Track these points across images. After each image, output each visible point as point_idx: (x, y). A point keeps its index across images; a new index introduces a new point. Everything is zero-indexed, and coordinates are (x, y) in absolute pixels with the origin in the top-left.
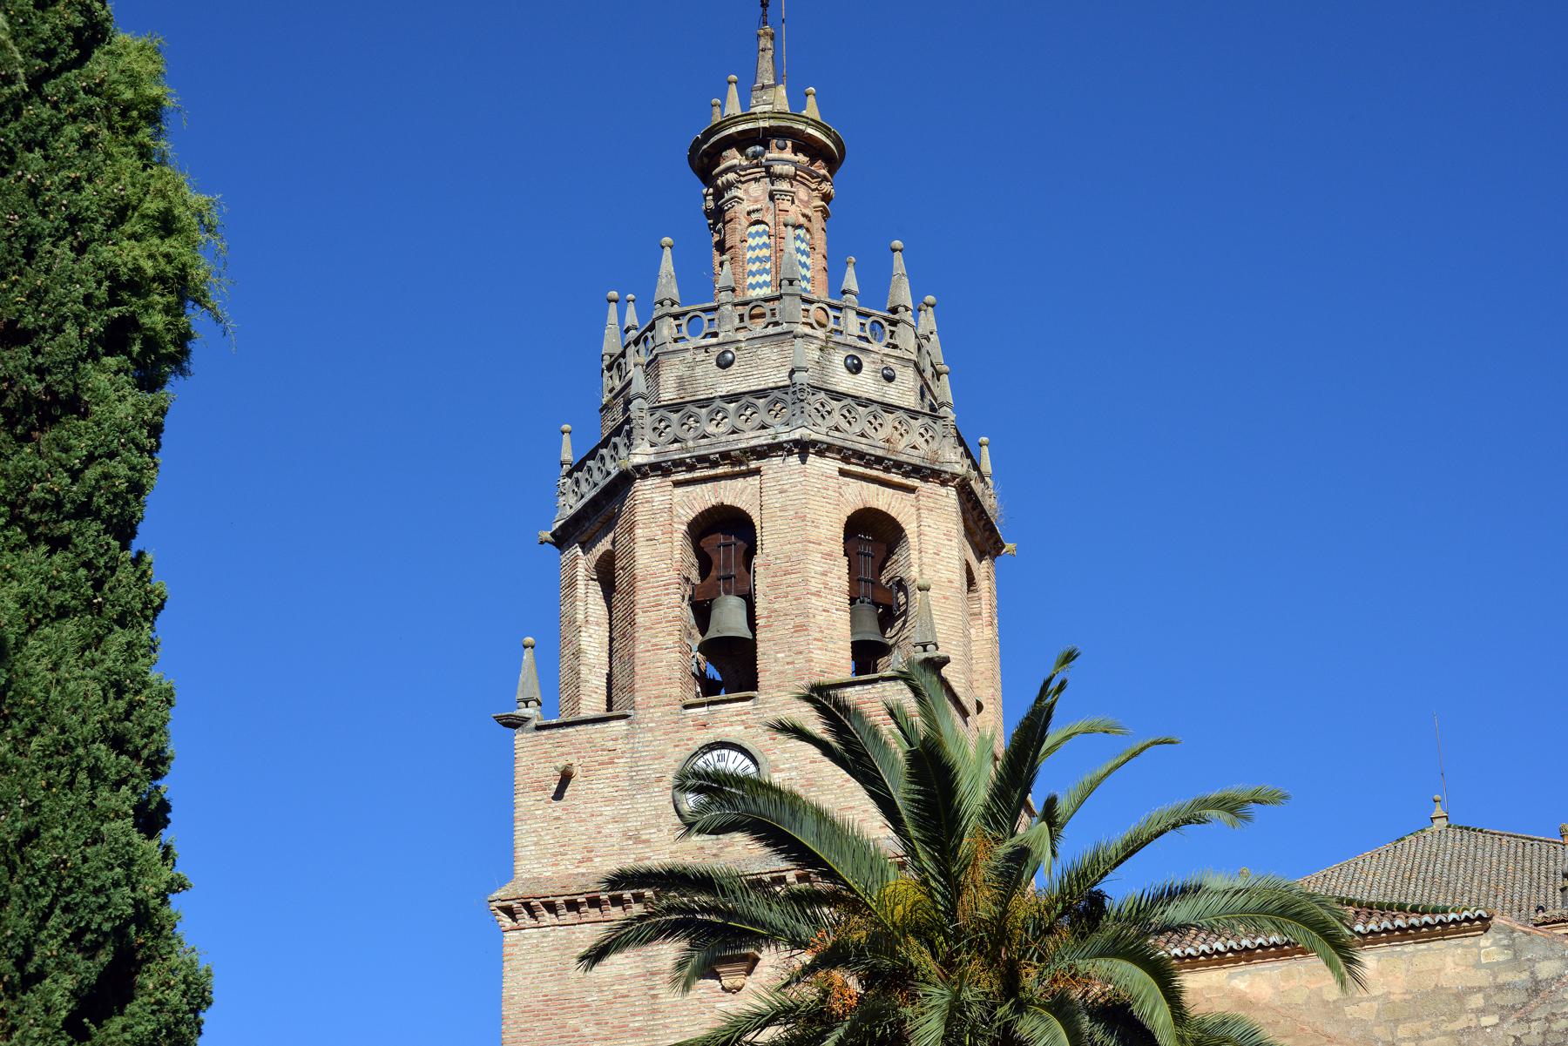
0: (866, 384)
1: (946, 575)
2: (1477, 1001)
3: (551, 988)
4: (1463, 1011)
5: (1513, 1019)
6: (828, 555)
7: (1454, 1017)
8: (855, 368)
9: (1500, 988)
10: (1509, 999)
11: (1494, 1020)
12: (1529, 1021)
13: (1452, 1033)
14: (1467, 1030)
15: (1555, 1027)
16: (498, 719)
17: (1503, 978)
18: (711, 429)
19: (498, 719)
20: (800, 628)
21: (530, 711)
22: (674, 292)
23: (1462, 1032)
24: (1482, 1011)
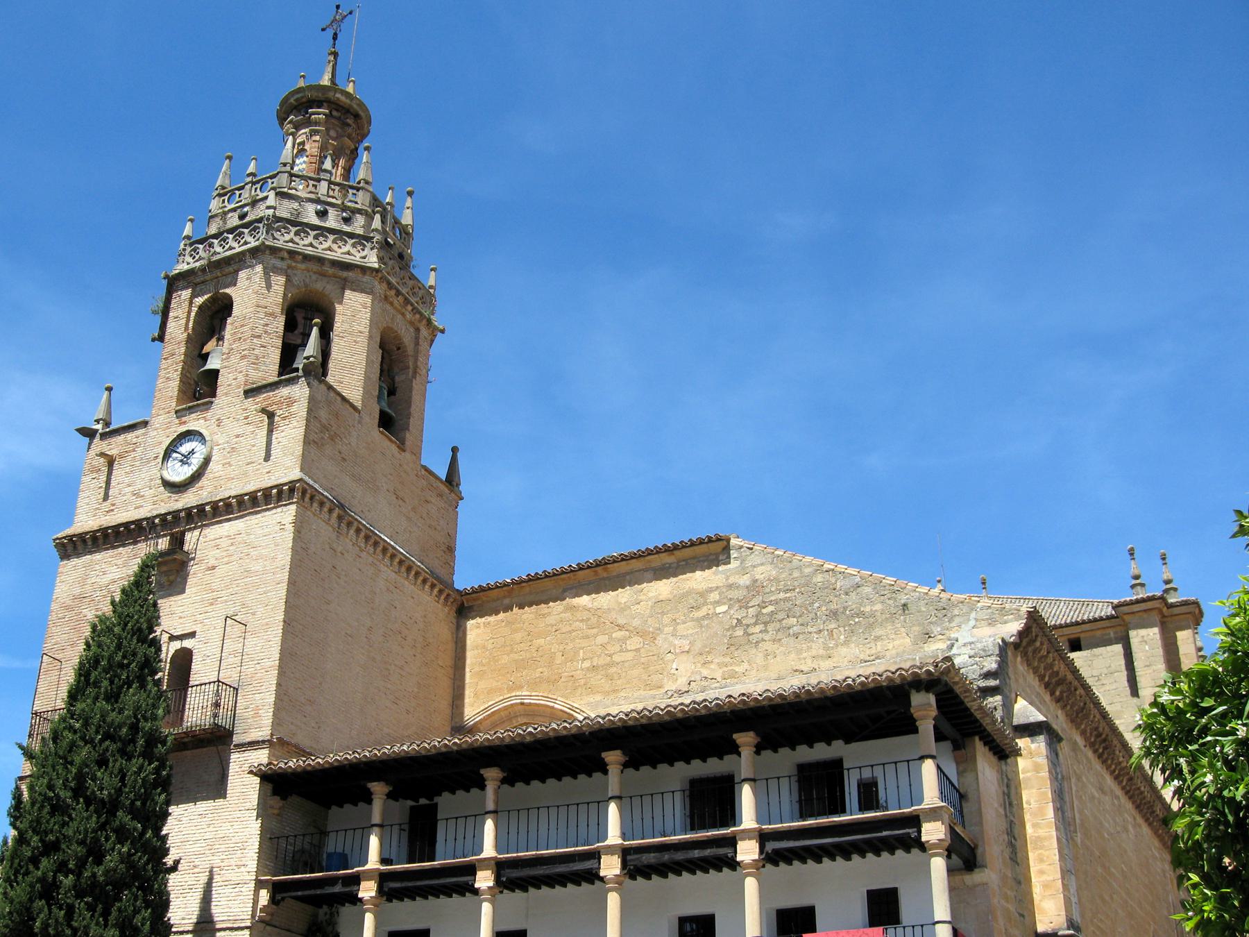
0: (332, 221)
1: (357, 328)
2: (714, 596)
3: (77, 591)
4: (705, 603)
5: (737, 606)
6: (271, 314)
7: (698, 608)
8: (322, 214)
9: (730, 586)
10: (735, 594)
11: (724, 608)
12: (747, 608)
13: (698, 620)
14: (707, 616)
15: (764, 611)
16: (78, 430)
17: (730, 581)
18: (218, 249)
19: (78, 430)
20: (244, 357)
21: (99, 427)
22: (227, 182)
23: (704, 618)
24: (718, 603)
